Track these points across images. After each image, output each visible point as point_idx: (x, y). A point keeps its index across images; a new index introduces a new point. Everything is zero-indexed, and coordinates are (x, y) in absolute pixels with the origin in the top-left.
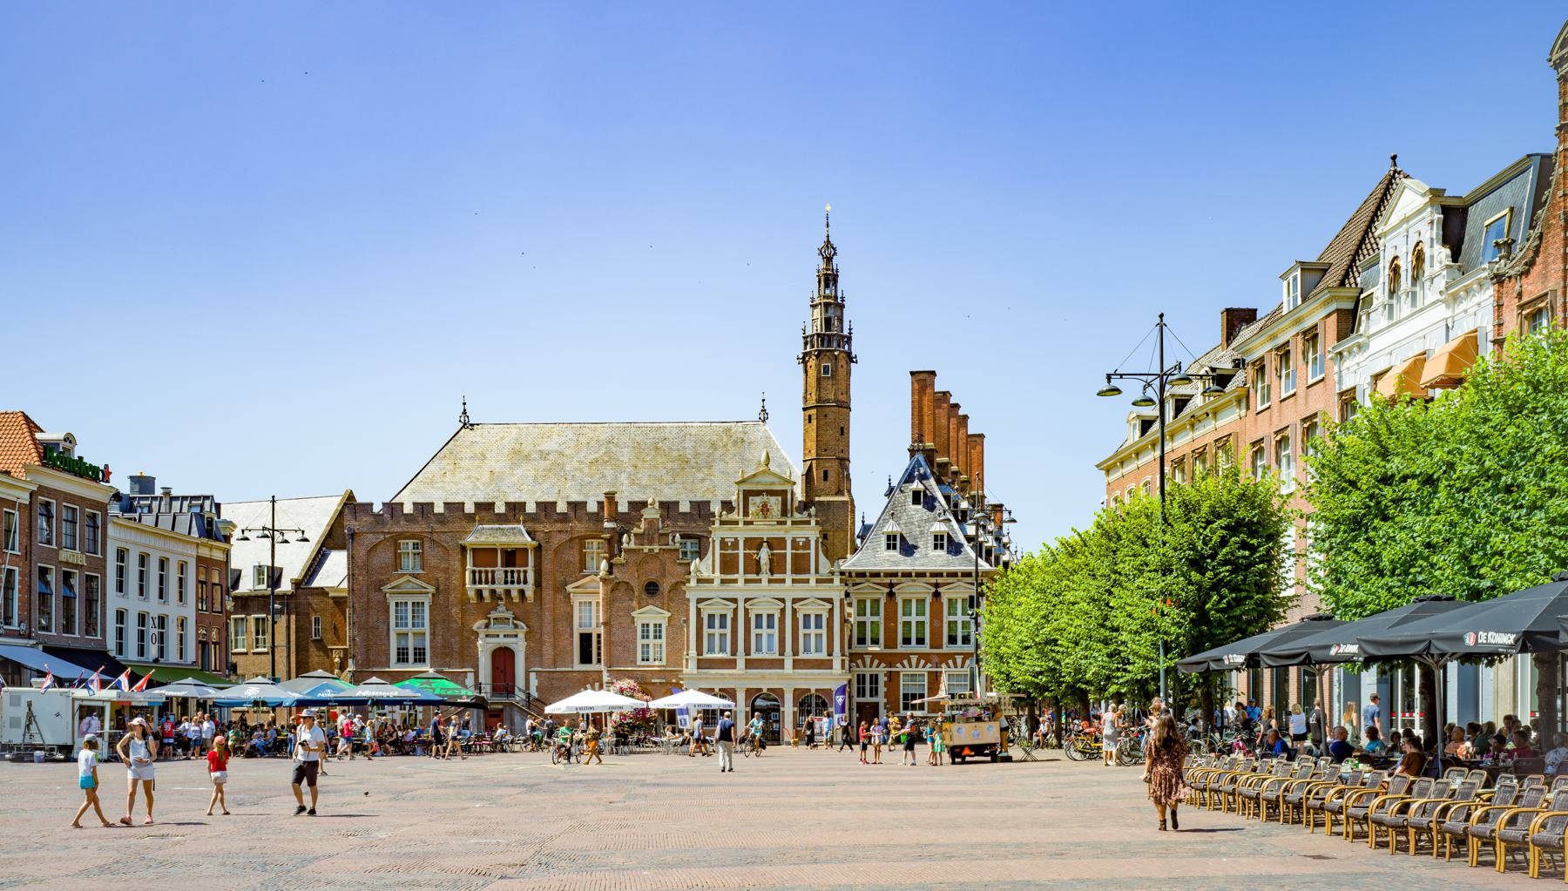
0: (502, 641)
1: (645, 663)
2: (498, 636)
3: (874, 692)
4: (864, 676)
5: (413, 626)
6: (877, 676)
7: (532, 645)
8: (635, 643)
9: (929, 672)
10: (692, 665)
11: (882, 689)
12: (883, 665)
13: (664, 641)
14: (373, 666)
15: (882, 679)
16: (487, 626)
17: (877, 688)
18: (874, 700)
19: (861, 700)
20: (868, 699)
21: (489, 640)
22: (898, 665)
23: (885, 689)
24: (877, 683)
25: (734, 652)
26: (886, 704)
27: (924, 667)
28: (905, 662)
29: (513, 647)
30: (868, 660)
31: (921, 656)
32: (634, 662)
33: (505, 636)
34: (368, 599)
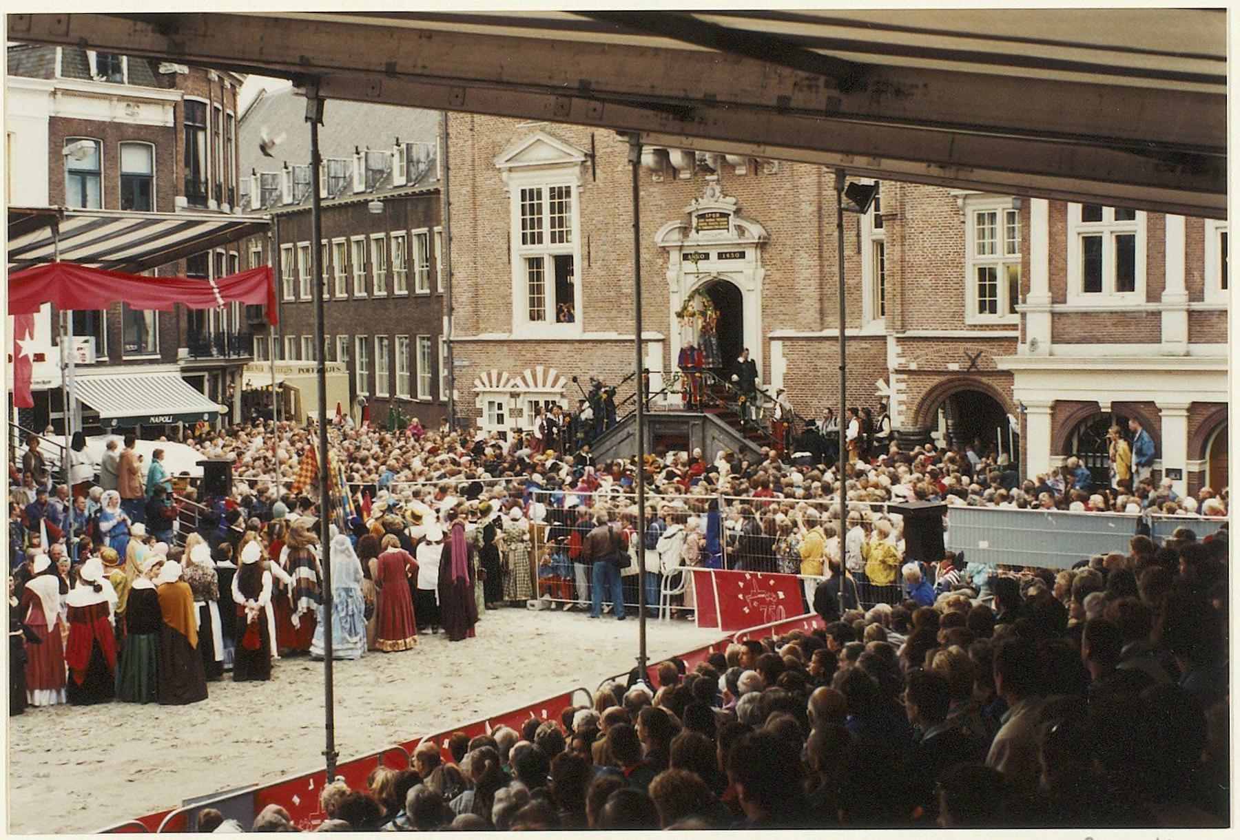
0: (714, 267)
1: (987, 318)
2: (707, 256)
5: (553, 241)
7: (777, 276)
8: (961, 265)
10: (1039, 327)
13: (973, 260)
14: (494, 330)
16: (685, 230)
21: (689, 266)
25: (1154, 294)
29: (737, 280)
32: (959, 316)
33: (720, 256)
34: (474, 187)
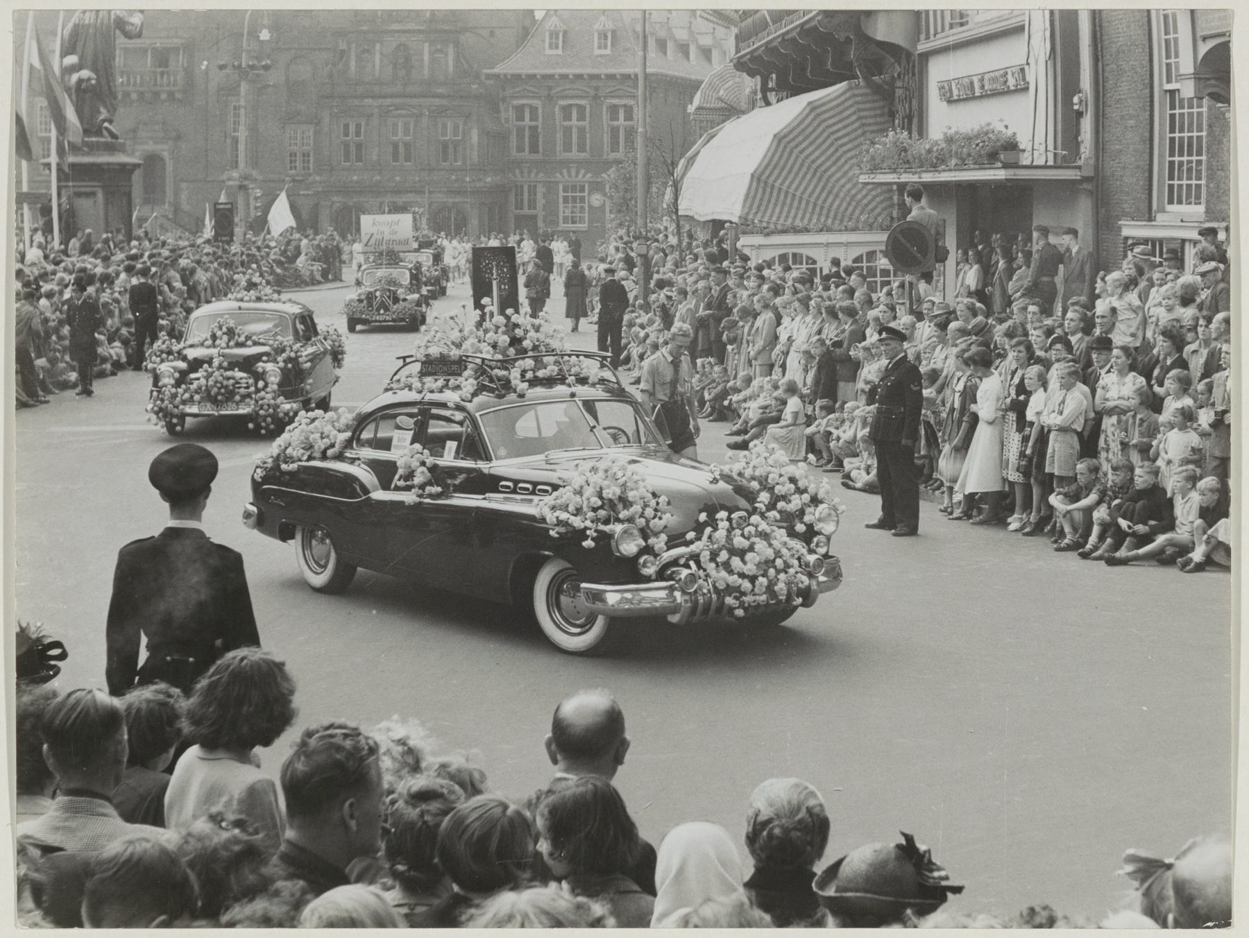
3: (532, 205)
4: (522, 187)
6: (535, 186)
9: (589, 182)
11: (541, 201)
12: (541, 175)
15: (541, 190)
17: (535, 200)
18: (532, 212)
19: (522, 212)
20: (526, 211)
22: (558, 175)
23: (544, 202)
24: (535, 195)
26: (545, 217)
27: (584, 176)
28: (565, 171)
30: (526, 171)
31: (580, 164)
